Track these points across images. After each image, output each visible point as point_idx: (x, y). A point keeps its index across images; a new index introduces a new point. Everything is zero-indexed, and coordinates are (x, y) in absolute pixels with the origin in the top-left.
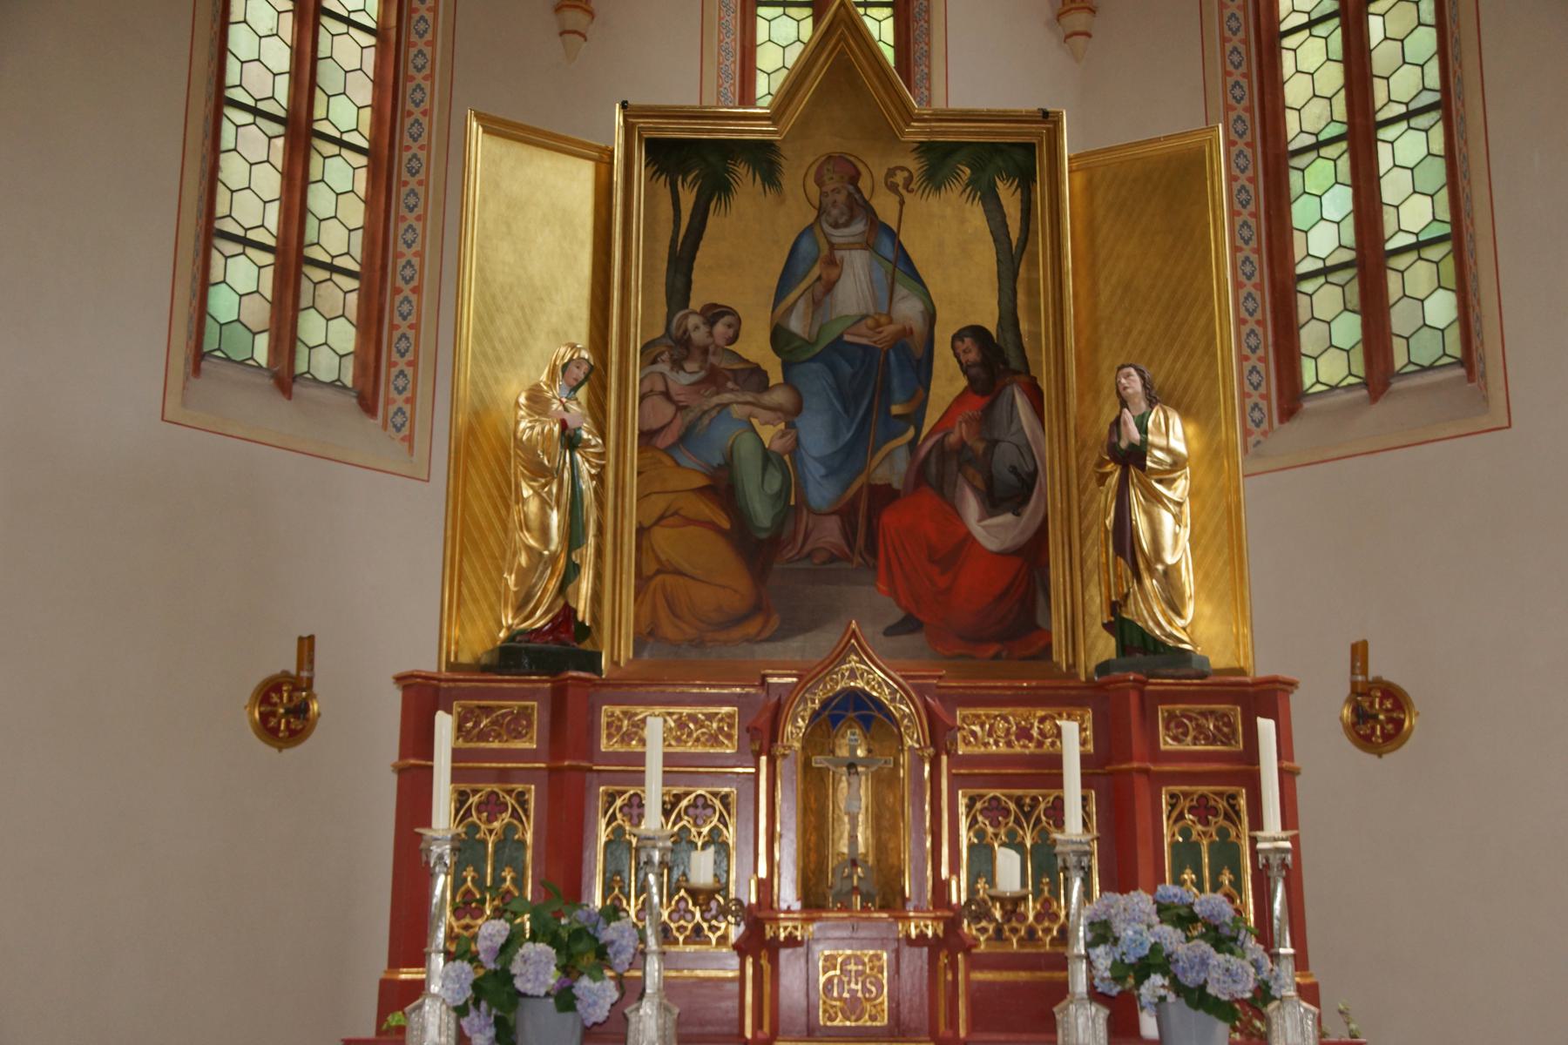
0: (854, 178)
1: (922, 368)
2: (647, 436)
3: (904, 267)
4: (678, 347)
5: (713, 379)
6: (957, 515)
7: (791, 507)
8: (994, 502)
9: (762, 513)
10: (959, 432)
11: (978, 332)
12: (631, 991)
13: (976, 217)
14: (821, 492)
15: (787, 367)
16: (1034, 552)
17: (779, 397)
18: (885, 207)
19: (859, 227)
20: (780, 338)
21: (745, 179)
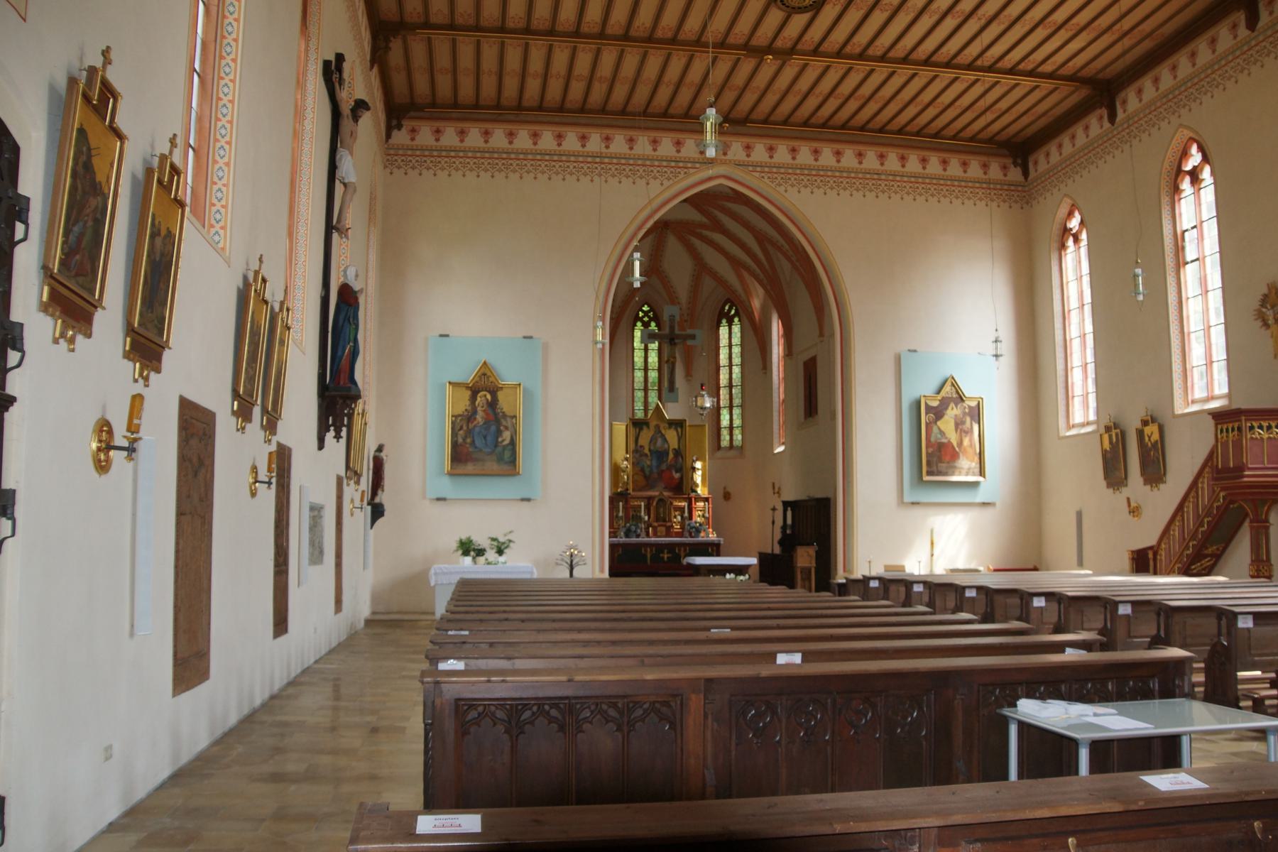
0: (659, 428)
1: (668, 454)
2: (633, 463)
3: (665, 440)
4: (635, 451)
5: (641, 456)
6: (672, 474)
7: (651, 472)
8: (677, 472)
9: (647, 473)
10: (673, 462)
11: (675, 449)
12: (641, 531)
13: (675, 433)
14: (655, 470)
15: (651, 454)
16: (681, 478)
17: (649, 458)
18: (663, 432)
19: (660, 434)
20: (650, 450)
21: (645, 427)
